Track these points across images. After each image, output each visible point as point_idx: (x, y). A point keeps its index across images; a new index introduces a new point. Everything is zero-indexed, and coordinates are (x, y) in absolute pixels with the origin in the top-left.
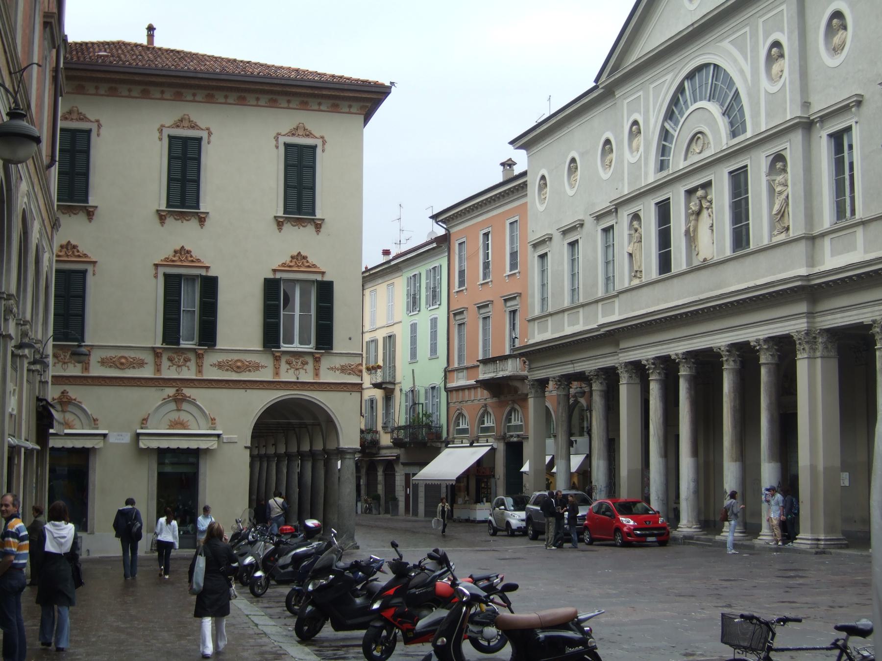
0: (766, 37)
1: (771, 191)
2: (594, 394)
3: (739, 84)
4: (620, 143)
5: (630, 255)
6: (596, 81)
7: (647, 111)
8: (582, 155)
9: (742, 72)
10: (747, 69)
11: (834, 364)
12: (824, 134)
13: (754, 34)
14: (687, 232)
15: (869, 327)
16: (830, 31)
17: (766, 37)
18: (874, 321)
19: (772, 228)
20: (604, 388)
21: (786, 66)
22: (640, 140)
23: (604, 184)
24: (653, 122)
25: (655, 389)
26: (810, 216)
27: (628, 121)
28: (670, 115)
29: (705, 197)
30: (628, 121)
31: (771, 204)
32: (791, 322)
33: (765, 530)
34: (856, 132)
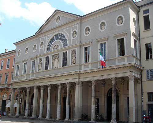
0: (73, 30)
1: (72, 56)
2: (49, 90)
3: (66, 37)
4: (38, 46)
5: (39, 66)
6: (35, 34)
7: (45, 41)
8: (29, 47)
9: (67, 36)
10: (68, 35)
11: (82, 88)
12: (84, 47)
13: (70, 30)
14: (52, 62)
15: (91, 81)
16: (86, 30)
17: (73, 30)
18: (93, 80)
19: (72, 63)
20: (43, 89)
21: (77, 36)
22: (43, 46)
23: (33, 53)
24: (47, 43)
25: (42, 91)
26: (80, 61)
27: (72, 31)
28: (50, 42)
29: (57, 57)
30: (72, 31)
31: (72, 59)
32: (75, 80)
33: (92, 119)
34: (90, 48)
